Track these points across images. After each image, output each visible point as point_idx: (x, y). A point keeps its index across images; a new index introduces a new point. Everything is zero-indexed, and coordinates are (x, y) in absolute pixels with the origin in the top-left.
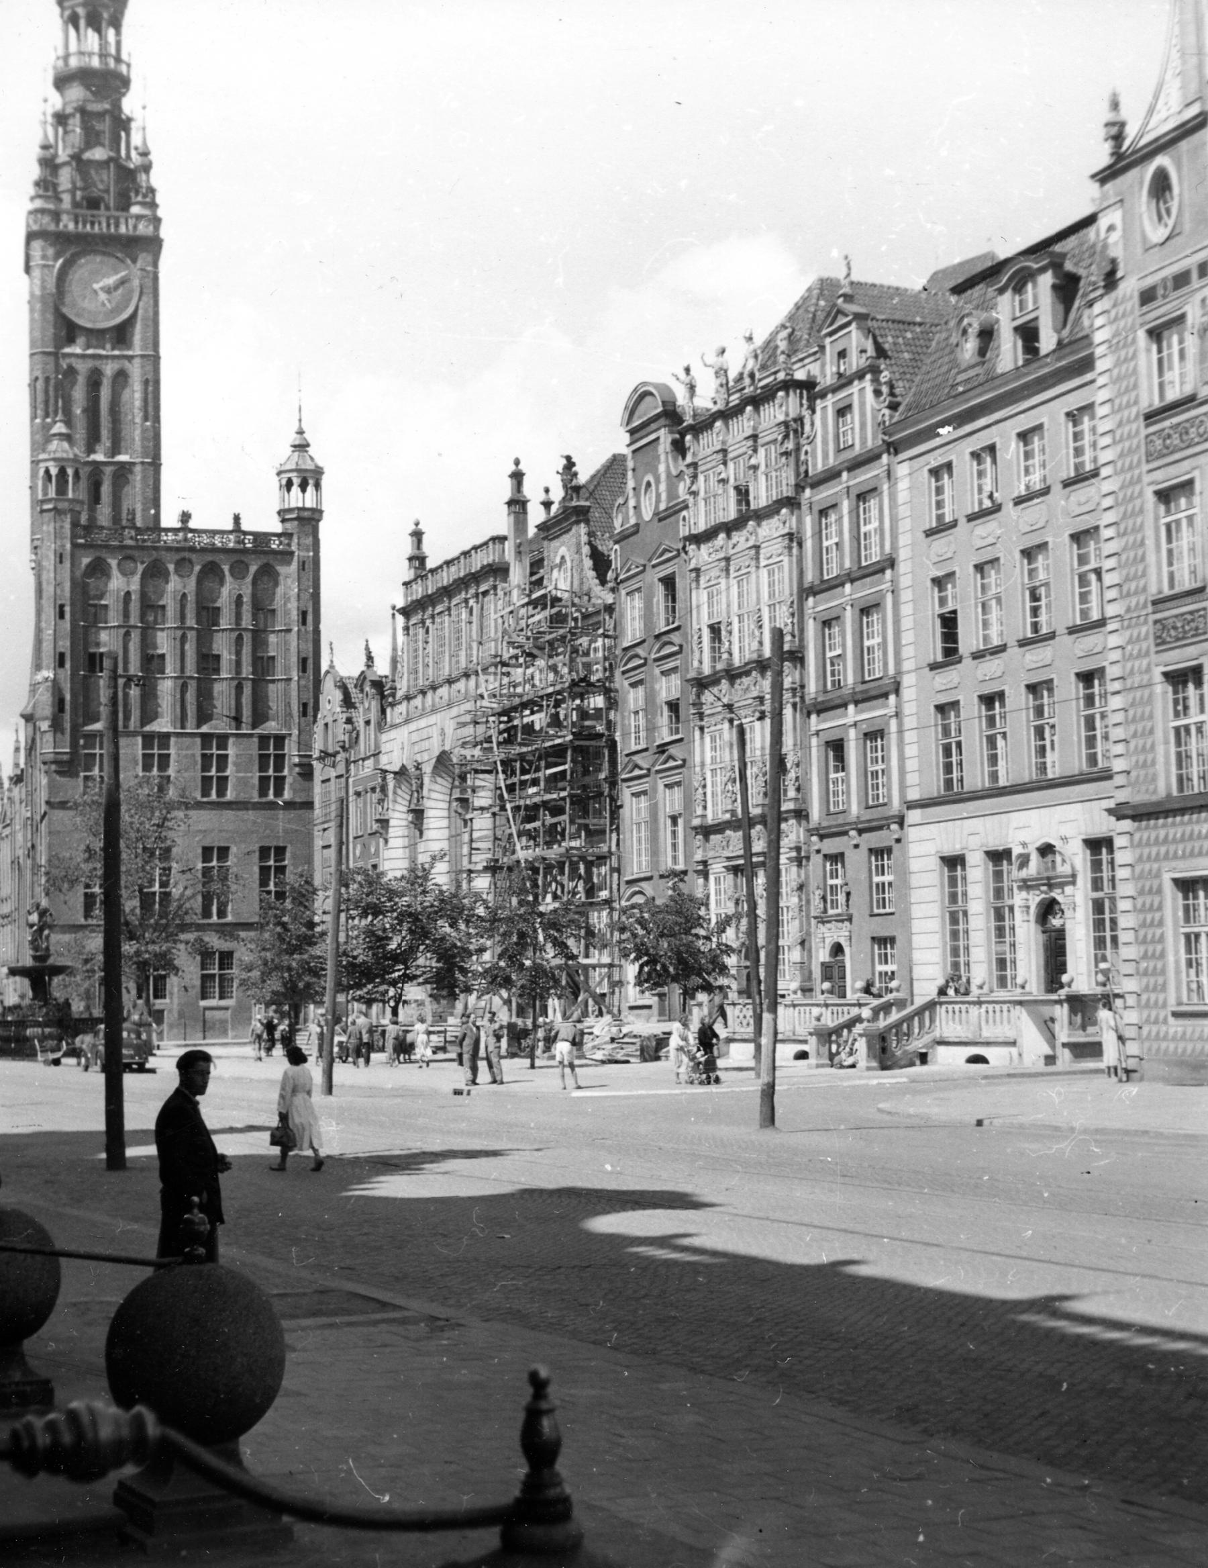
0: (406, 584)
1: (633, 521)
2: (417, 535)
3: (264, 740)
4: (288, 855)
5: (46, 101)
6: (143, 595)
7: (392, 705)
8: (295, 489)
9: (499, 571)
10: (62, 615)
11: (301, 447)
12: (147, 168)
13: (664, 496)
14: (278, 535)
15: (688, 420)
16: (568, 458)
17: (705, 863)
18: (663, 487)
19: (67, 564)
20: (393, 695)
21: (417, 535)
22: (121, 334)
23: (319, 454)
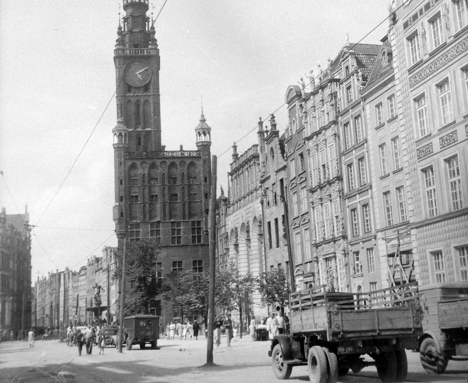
0: (231, 164)
1: (290, 135)
2: (235, 147)
3: (193, 223)
4: (203, 264)
5: (119, 14)
6: (149, 174)
7: (229, 207)
8: (203, 135)
9: (256, 157)
10: (121, 184)
11: (203, 121)
12: (154, 33)
13: (298, 125)
14: (196, 151)
15: (303, 97)
16: (272, 115)
17: (317, 257)
18: (298, 121)
19: (123, 166)
20: (229, 204)
21: (235, 147)
22: (146, 88)
23: (209, 123)
